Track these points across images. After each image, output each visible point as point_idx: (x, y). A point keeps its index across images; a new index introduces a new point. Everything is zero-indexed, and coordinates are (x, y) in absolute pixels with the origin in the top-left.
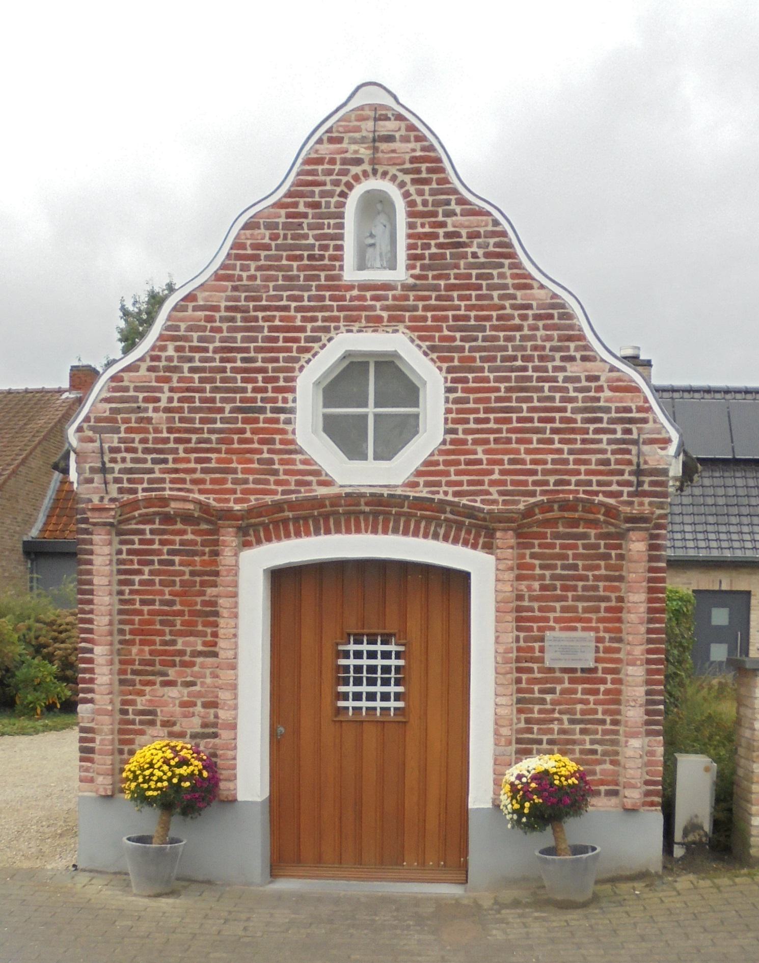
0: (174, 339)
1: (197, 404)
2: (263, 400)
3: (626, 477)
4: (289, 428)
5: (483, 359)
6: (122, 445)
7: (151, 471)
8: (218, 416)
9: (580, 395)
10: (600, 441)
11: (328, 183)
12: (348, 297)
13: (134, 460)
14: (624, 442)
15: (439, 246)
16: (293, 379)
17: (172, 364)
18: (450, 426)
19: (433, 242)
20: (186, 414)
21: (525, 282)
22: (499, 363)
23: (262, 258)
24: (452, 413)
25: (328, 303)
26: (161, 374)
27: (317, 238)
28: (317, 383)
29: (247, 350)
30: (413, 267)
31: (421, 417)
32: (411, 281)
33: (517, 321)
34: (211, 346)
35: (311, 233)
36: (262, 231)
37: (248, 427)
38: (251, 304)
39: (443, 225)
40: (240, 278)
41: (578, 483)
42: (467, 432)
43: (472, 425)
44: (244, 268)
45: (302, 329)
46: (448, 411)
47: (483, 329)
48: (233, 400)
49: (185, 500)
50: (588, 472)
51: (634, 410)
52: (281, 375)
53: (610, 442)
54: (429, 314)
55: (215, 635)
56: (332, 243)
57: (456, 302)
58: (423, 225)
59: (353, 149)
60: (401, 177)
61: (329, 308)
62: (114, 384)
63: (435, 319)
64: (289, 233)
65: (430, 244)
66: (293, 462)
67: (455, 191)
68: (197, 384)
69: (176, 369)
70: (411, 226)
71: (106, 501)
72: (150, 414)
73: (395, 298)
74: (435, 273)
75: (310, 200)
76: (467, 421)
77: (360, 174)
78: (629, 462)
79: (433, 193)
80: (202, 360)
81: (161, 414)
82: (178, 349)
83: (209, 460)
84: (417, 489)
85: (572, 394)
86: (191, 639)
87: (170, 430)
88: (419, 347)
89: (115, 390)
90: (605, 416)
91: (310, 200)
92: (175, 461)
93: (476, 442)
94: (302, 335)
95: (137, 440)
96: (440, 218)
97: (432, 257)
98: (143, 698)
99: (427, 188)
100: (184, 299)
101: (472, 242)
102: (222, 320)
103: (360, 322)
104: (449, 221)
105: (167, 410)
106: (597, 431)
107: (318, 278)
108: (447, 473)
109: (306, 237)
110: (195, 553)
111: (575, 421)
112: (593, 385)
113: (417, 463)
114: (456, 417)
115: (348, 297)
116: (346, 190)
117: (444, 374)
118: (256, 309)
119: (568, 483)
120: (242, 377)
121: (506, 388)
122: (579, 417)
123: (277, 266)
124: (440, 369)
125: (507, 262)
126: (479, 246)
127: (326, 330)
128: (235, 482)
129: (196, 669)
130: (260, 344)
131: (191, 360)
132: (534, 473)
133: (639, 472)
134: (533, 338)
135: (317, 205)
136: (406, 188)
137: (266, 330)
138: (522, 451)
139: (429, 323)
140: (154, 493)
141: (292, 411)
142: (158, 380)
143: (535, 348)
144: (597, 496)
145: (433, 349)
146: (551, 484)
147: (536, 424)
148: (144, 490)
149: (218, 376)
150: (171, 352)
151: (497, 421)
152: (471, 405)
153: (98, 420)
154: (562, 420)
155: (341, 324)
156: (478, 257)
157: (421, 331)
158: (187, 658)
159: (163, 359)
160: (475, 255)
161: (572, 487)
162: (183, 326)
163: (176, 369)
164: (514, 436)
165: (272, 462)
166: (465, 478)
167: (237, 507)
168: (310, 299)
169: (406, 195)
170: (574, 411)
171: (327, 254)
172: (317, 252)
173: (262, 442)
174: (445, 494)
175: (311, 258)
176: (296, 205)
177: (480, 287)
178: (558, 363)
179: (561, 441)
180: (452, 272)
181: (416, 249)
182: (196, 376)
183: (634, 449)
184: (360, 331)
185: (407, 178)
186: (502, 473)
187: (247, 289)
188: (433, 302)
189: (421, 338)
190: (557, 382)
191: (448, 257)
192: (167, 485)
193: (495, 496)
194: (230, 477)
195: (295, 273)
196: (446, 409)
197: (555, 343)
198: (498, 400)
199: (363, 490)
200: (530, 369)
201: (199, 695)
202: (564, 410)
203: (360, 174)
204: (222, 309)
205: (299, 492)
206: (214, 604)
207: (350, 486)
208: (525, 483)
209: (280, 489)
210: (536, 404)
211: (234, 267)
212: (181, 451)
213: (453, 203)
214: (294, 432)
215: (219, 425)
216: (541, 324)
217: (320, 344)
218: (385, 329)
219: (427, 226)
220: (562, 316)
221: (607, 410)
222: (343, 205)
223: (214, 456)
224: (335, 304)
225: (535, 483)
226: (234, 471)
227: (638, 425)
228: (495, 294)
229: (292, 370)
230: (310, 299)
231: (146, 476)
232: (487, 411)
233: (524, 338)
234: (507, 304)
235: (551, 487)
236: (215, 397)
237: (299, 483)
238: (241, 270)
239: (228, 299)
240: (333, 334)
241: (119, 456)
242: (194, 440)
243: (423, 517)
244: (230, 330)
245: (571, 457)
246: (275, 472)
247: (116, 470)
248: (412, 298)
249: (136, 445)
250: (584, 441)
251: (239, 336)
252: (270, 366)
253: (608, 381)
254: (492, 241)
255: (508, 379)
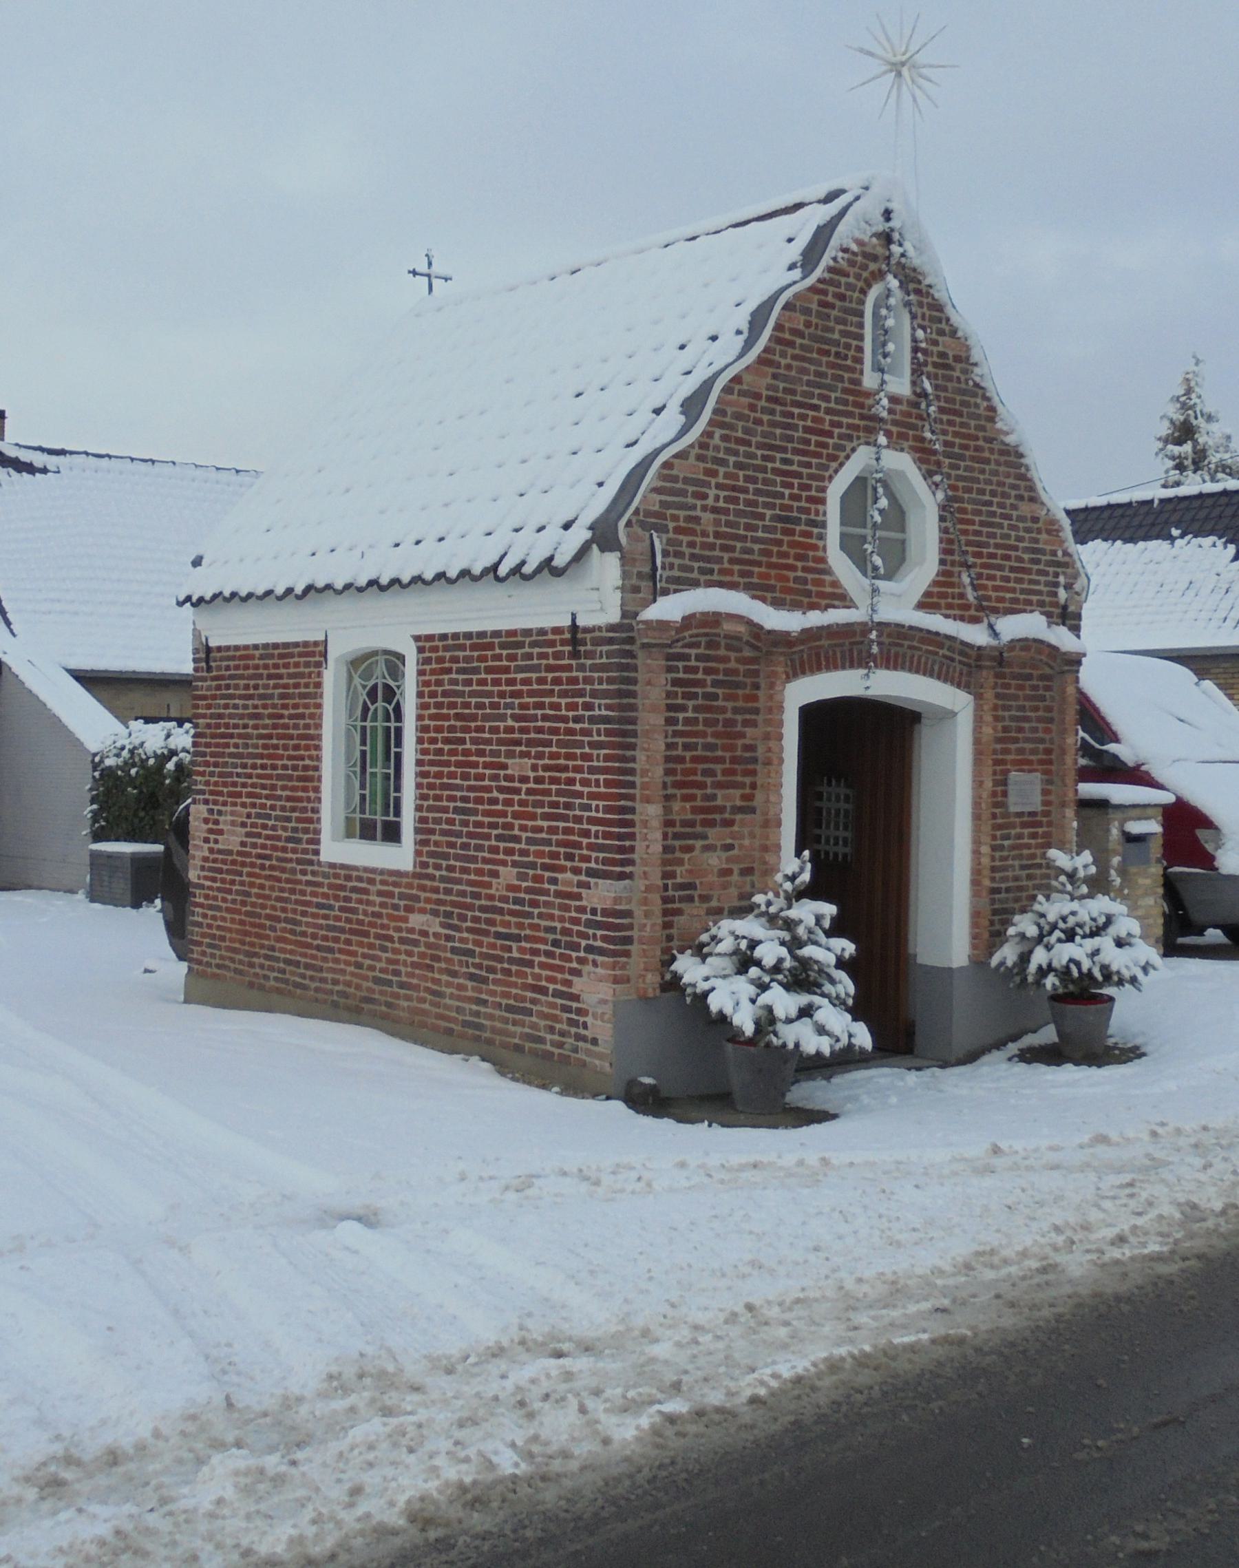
0: (722, 425)
4: (820, 543)
16: (824, 490)
33: (986, 454)
55: (753, 786)
56: (854, 343)
62: (665, 472)
68: (741, 483)
69: (723, 462)
72: (698, 513)
82: (725, 438)
83: (749, 574)
86: (731, 791)
87: (717, 535)
98: (683, 868)
100: (731, 380)
105: (715, 510)
109: (832, 330)
110: (737, 685)
122: (1026, 556)
127: (850, 438)
129: (736, 828)
135: (842, 297)
150: (716, 440)
153: (648, 514)
158: (727, 816)
163: (723, 462)
187: (786, 379)
201: (736, 860)
206: (750, 748)
212: (725, 560)
214: (824, 549)
215: (760, 534)
222: (863, 303)
228: (973, 423)
229: (822, 479)
240: (855, 443)
243: (928, 651)
249: (684, 549)
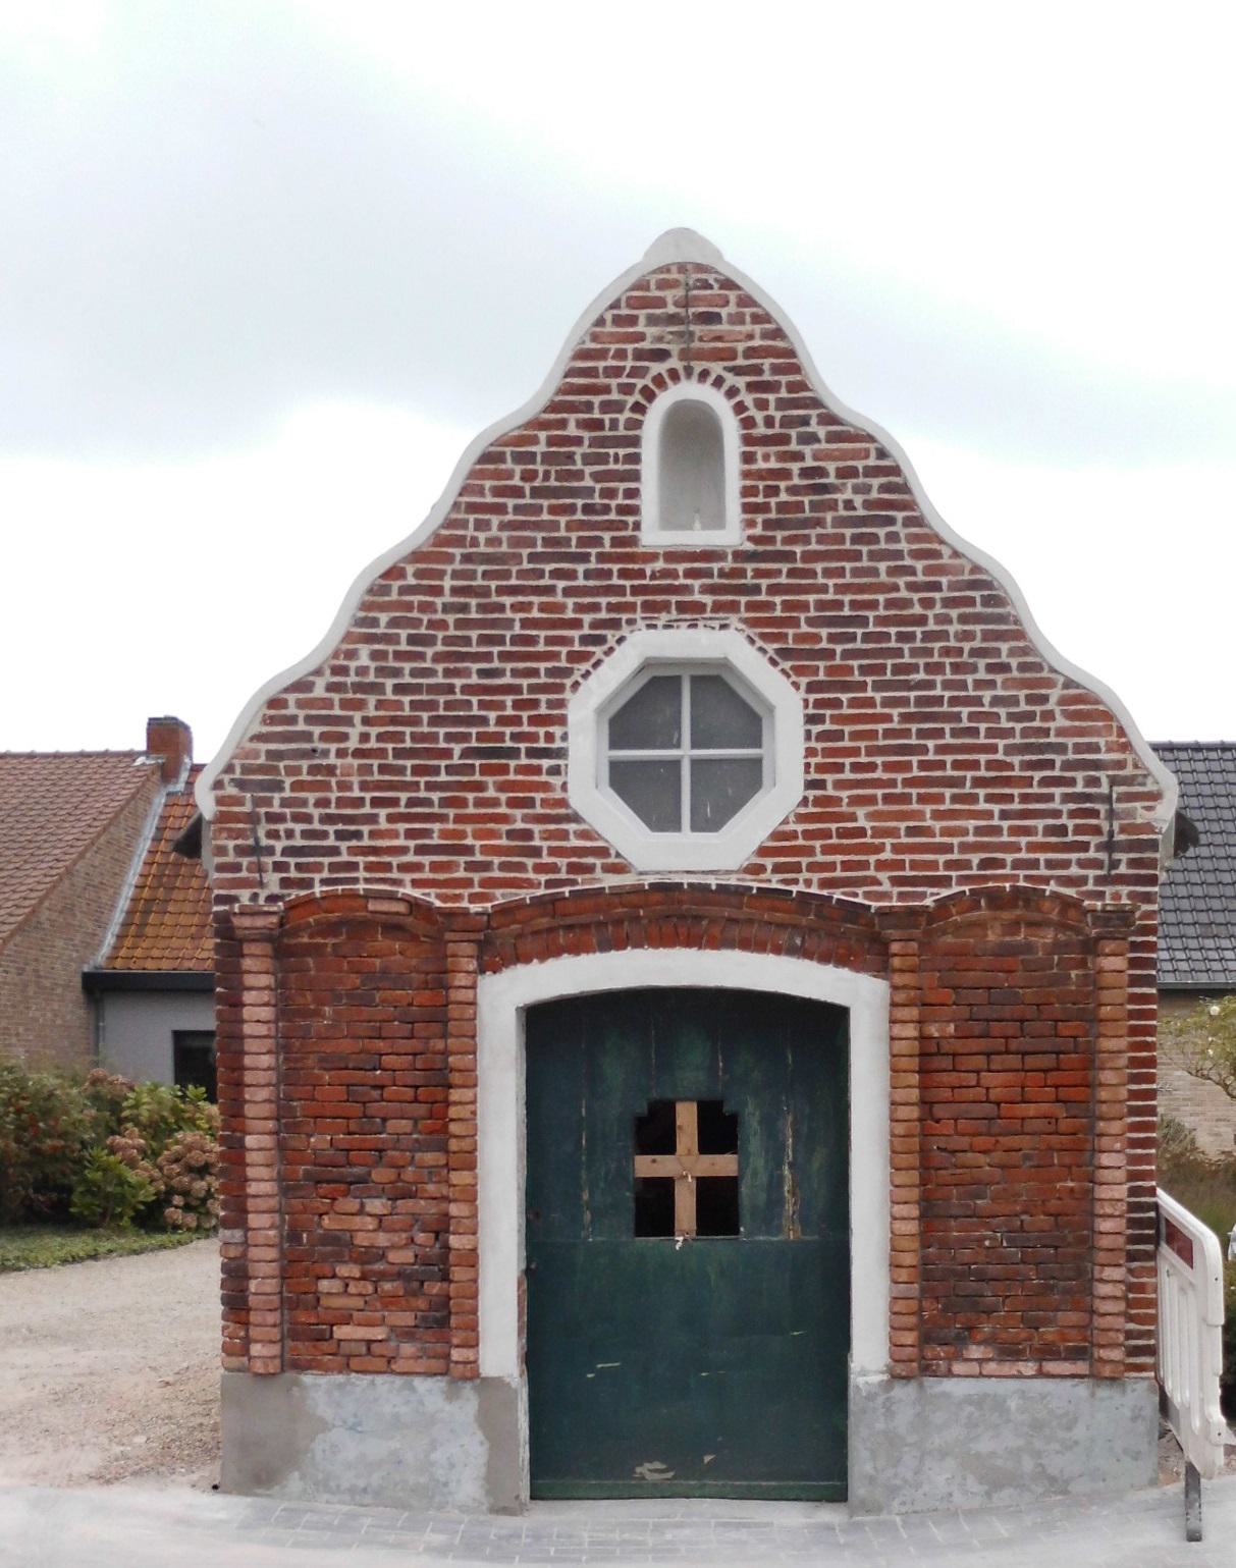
0: (370, 639)
1: (408, 744)
2: (515, 737)
3: (1092, 854)
4: (556, 781)
5: (864, 670)
6: (287, 811)
7: (335, 851)
8: (443, 763)
9: (1018, 726)
10: (1050, 798)
11: (614, 388)
12: (648, 573)
13: (306, 834)
14: (1087, 798)
15: (792, 490)
16: (561, 704)
17: (367, 681)
18: (814, 776)
19: (783, 485)
20: (391, 760)
21: (930, 543)
22: (889, 676)
23: (510, 510)
24: (816, 755)
25: (615, 581)
26: (350, 695)
27: (598, 477)
28: (600, 711)
29: (488, 657)
30: (751, 524)
31: (765, 763)
32: (749, 546)
33: (917, 610)
34: (430, 652)
35: (588, 470)
36: (509, 465)
37: (490, 780)
38: (493, 584)
39: (798, 457)
40: (475, 542)
41: (1017, 864)
42: (839, 785)
43: (848, 775)
44: (481, 525)
45: (576, 624)
46: (810, 752)
47: (864, 621)
48: (466, 737)
49: (391, 897)
50: (1032, 847)
51: (1103, 749)
52: (543, 698)
53: (1067, 798)
54: (778, 599)
56: (622, 486)
57: (821, 580)
58: (766, 457)
59: (651, 335)
60: (731, 380)
61: (620, 591)
62: (273, 712)
63: (787, 606)
64: (553, 469)
65: (777, 487)
66: (564, 835)
67: (816, 403)
68: (407, 712)
69: (376, 688)
70: (748, 458)
71: (261, 901)
72: (332, 760)
73: (722, 574)
74: (787, 533)
75: (587, 416)
76: (839, 768)
77: (666, 376)
78: (1097, 830)
79: (782, 404)
80: (414, 673)
81: (350, 760)
82: (376, 656)
83: (427, 833)
84: (763, 876)
85: (1005, 724)
87: (364, 787)
88: (762, 650)
89: (272, 720)
90: (1058, 759)
91: (587, 416)
92: (373, 835)
93: (855, 801)
94: (575, 634)
95: (312, 801)
96: (794, 446)
97: (783, 507)
99: (771, 397)
101: (844, 484)
102: (446, 608)
103: (669, 612)
104: (807, 450)
105: (358, 753)
106: (1045, 782)
107: (598, 541)
108: (810, 851)
109: (579, 475)
111: (1011, 767)
112: (1038, 709)
113: (760, 836)
114: (825, 759)
115: (648, 573)
116: (644, 402)
117: (802, 694)
118: (501, 591)
119: (1001, 864)
120: (480, 701)
121: (900, 715)
122: (1016, 760)
123: (534, 523)
124: (796, 685)
125: (900, 515)
126: (857, 490)
127: (615, 624)
128: (470, 867)
130: (508, 648)
131: (397, 672)
132: (948, 849)
133: (1109, 846)
134: (942, 636)
135: (597, 425)
136: (738, 399)
137: (517, 625)
138: (928, 815)
139: (778, 613)
140: (340, 887)
141: (561, 753)
142: (345, 704)
143: (946, 652)
144: (1048, 884)
145: (785, 653)
146: (975, 867)
147: (950, 772)
148: (324, 882)
149: (442, 699)
150: (364, 660)
151: (888, 767)
152: (846, 743)
153: (246, 770)
154: (990, 765)
155: (639, 615)
156: (854, 509)
157: (767, 628)
159: (352, 673)
160: (849, 505)
161: (1007, 871)
162: (384, 618)
163: (376, 688)
164: (914, 791)
165: (527, 835)
166: (839, 858)
167: (475, 908)
168: (588, 575)
169: (740, 408)
170: (1009, 750)
171: (613, 503)
172: (597, 500)
173: (513, 803)
174: (806, 884)
175: (587, 509)
176: (563, 424)
177: (857, 556)
178: (982, 675)
179: (990, 799)
180: (814, 533)
181: (756, 496)
182: (406, 699)
183: (1102, 808)
184: (667, 627)
185: (741, 382)
186: (896, 849)
188: (783, 580)
189: (763, 636)
190: (983, 705)
191: (807, 507)
192: (362, 874)
193: (886, 887)
194: (462, 859)
195: (563, 533)
196: (807, 749)
197: (977, 644)
198: (888, 734)
199: (676, 879)
200: (939, 685)
202: (993, 749)
203: (666, 376)
204: (447, 591)
205: (574, 882)
207: (658, 873)
208: (934, 865)
209: (543, 878)
210: (948, 740)
211: (464, 524)
212: (382, 819)
213: (814, 421)
214: (564, 787)
215: (443, 777)
216: (954, 613)
217: (605, 647)
218: (709, 623)
219: (773, 458)
220: (988, 601)
221: (1061, 749)
222: (638, 424)
223: (436, 826)
224: (628, 583)
225: (949, 865)
226: (469, 850)
227: (1110, 773)
228: (883, 566)
229: (560, 688)
230: (588, 575)
231: (326, 860)
232: (870, 752)
233: (928, 636)
234: (901, 581)
235: (975, 872)
236: (437, 733)
237: (572, 868)
238: (476, 529)
239: (456, 575)
240: (625, 630)
241: (281, 827)
242: (403, 802)
244: (459, 624)
245: (1005, 824)
246: (536, 852)
247: (278, 850)
248: (750, 574)
249: (311, 810)
250: (1025, 798)
251: (474, 634)
252: (525, 682)
253: (1063, 701)
254: (876, 482)
255: (905, 702)
